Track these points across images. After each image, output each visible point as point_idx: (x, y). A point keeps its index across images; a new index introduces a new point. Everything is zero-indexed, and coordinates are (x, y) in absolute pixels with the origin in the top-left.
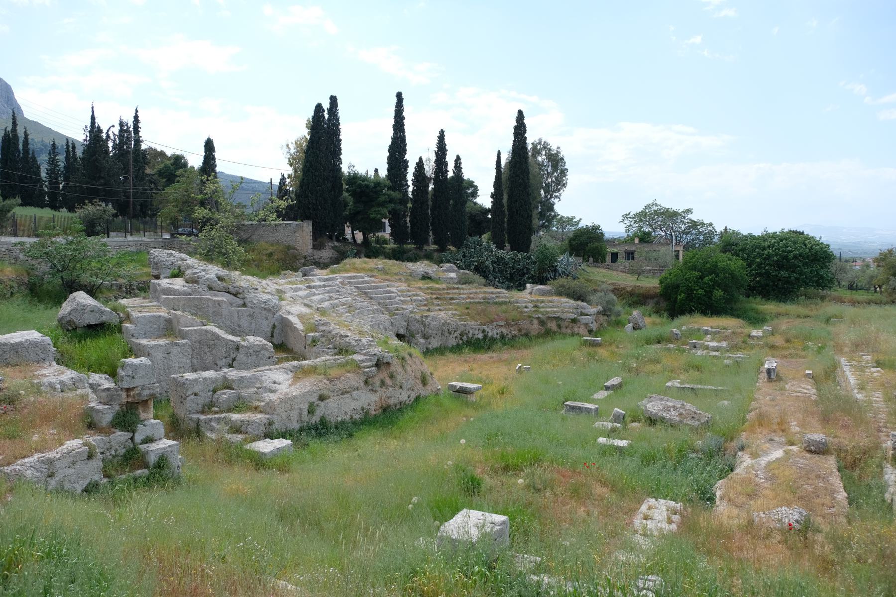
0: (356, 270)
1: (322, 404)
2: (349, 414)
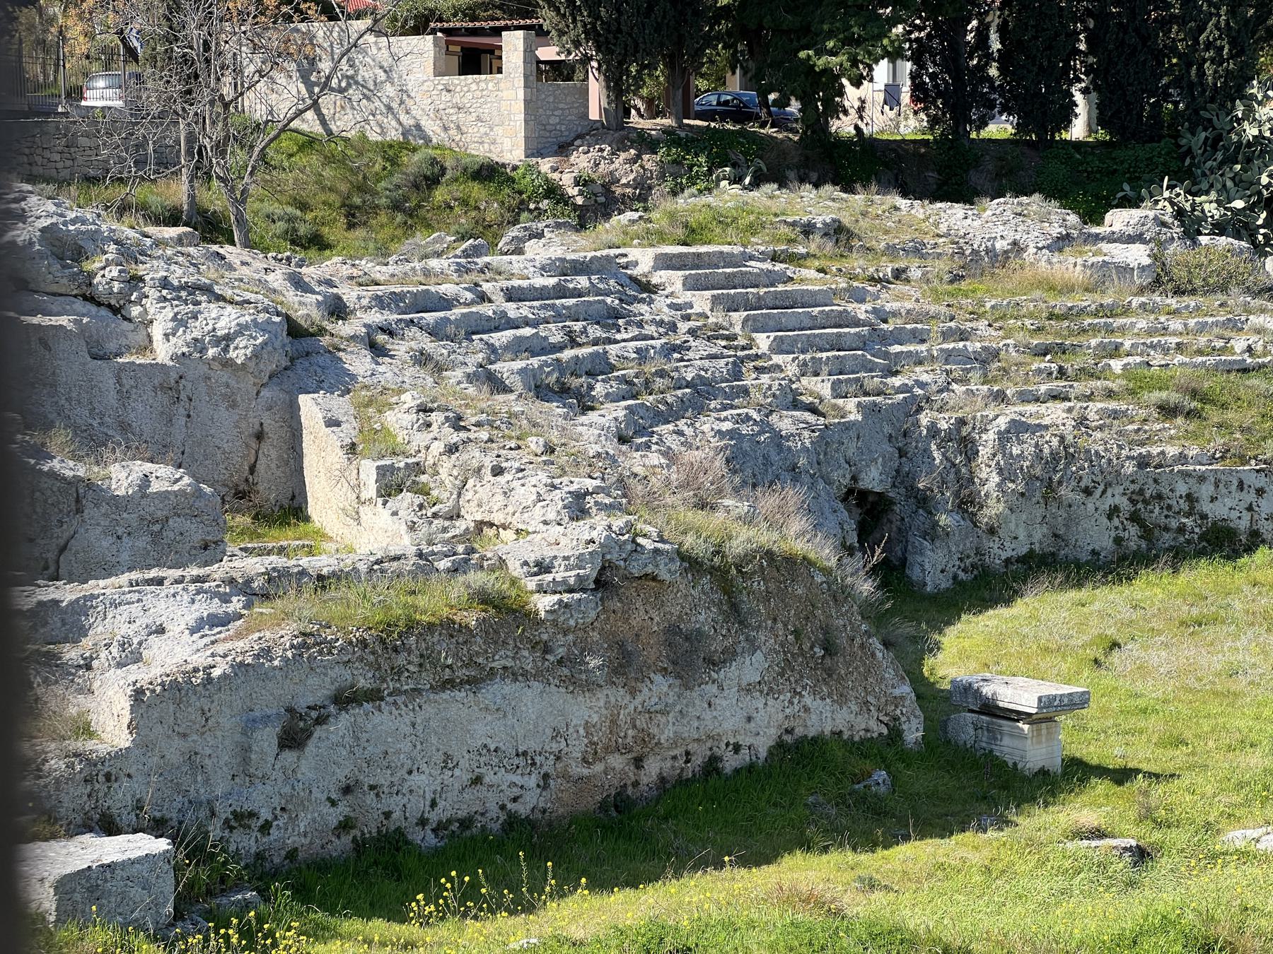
2: (464, 763)
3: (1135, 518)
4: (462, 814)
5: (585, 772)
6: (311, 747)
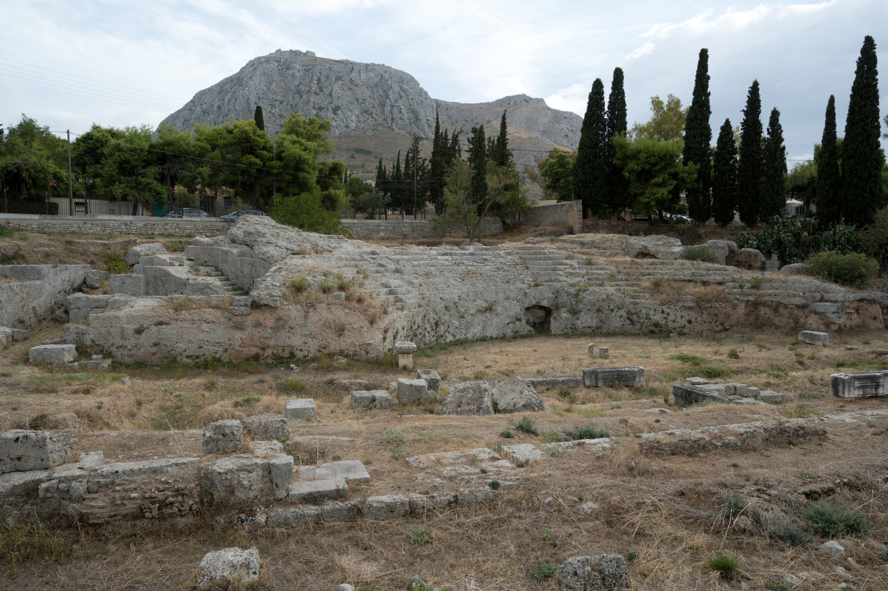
1: (154, 329)
3: (628, 319)
5: (241, 349)
6: (143, 334)
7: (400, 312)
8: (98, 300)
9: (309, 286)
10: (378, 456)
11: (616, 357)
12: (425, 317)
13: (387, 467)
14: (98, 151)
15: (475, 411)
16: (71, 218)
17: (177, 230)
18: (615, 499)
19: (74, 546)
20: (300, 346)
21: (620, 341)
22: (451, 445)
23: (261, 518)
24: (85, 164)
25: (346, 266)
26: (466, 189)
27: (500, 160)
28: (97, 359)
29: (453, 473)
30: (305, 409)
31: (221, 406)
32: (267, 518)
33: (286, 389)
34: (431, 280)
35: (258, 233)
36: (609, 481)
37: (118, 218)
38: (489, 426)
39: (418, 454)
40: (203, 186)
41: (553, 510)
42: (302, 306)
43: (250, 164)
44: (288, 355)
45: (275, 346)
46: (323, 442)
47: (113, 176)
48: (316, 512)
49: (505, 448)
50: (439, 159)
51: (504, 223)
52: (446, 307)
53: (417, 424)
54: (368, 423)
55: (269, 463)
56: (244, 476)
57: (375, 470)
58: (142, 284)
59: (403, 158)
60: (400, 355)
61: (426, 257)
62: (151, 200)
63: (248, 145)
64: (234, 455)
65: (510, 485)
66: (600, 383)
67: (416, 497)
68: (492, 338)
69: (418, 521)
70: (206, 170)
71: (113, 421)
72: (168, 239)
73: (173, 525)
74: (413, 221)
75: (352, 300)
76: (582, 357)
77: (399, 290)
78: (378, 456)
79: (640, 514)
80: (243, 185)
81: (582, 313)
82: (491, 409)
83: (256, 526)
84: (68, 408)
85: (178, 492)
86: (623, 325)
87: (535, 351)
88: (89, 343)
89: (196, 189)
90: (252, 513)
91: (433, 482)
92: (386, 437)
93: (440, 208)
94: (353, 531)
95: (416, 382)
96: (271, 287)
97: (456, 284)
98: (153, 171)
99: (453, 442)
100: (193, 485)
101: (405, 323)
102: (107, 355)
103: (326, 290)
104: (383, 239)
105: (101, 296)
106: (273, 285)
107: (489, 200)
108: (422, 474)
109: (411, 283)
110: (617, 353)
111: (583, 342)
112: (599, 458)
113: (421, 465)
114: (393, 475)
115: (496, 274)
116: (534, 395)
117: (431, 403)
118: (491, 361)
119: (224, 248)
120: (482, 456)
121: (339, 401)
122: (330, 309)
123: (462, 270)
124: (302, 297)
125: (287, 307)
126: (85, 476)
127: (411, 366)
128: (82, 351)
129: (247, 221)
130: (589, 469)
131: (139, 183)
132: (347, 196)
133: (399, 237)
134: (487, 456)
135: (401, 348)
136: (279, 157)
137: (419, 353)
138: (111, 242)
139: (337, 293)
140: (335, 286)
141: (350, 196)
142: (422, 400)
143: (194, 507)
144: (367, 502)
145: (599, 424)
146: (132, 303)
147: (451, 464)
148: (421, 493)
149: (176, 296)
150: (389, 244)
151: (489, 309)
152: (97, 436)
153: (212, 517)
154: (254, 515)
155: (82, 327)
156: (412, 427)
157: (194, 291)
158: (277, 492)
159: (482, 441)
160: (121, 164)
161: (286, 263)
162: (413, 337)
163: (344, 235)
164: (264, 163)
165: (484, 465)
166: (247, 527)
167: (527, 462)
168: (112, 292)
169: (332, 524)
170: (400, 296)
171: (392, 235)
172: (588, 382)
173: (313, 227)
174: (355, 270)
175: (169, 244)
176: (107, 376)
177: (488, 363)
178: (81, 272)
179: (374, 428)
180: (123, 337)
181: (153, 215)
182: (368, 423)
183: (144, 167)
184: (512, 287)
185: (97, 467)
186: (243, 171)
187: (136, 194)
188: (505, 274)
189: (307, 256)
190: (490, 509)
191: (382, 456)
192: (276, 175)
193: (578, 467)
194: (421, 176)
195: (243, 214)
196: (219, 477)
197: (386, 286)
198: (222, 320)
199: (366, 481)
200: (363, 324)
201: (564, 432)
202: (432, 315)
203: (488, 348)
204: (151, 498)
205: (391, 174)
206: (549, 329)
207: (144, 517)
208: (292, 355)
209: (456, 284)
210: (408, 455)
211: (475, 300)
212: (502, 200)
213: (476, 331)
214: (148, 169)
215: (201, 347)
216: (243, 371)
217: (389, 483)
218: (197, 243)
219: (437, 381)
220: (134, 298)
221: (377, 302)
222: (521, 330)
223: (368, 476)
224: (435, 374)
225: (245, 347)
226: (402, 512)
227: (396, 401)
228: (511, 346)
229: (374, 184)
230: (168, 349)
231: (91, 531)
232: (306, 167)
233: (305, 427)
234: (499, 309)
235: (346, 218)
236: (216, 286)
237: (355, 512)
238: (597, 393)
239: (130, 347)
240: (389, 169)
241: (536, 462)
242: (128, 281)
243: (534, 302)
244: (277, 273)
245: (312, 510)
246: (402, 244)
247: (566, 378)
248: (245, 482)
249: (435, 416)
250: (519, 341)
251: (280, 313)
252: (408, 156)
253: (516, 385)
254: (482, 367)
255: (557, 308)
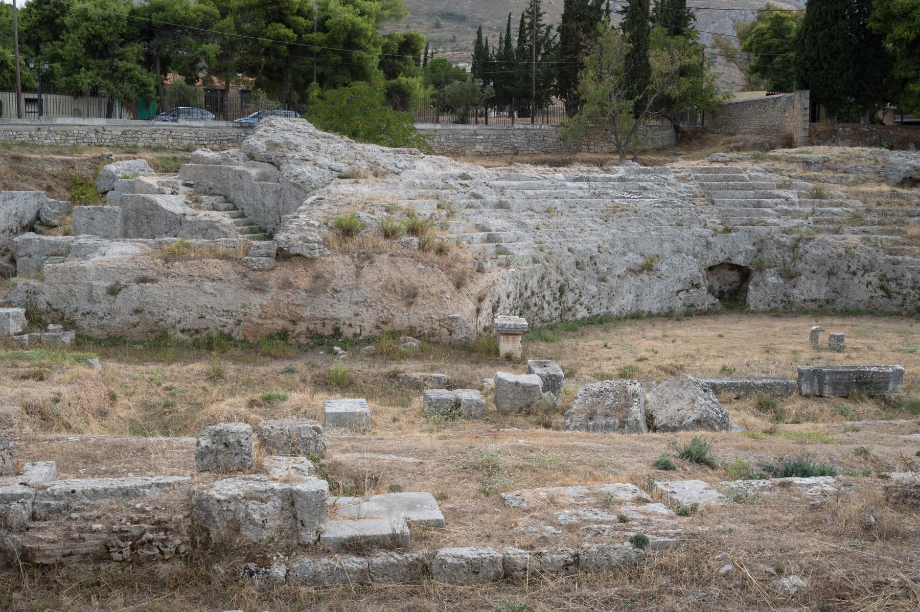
0: (776, 158)
1: (135, 287)
3: (882, 288)
4: (196, 327)
5: (260, 322)
6: (120, 295)
7: (503, 270)
8: (56, 244)
9: (364, 226)
10: (458, 488)
11: (856, 350)
12: (543, 278)
13: (471, 505)
14: (58, 21)
15: (616, 426)
16: (20, 121)
17: (170, 140)
18: (838, 573)
19: (15, 595)
20: (349, 319)
21: (865, 323)
22: (574, 476)
23: (279, 571)
24: (39, 40)
25: (421, 196)
26: (617, 74)
27: (673, 26)
28: (54, 331)
29: (574, 520)
30: (353, 414)
31: (230, 405)
32: (288, 571)
33: (326, 384)
34: (554, 220)
35: (288, 143)
36: (829, 545)
37: (86, 122)
38: (636, 451)
39: (521, 487)
40: (210, 72)
41: (732, 585)
42: (353, 257)
43: (279, 39)
44: (331, 332)
45: (313, 318)
46: (375, 463)
47: (77, 58)
48: (360, 567)
49: (660, 485)
50: (574, 25)
51: (677, 129)
52: (577, 264)
53: (521, 442)
54: (446, 438)
55: (291, 490)
56: (255, 507)
57: (453, 509)
58: (119, 220)
59: (515, 26)
60: (502, 338)
61: (547, 183)
62: (133, 95)
63: (275, 7)
64: (240, 475)
65: (665, 542)
66: (827, 391)
67: (514, 552)
68: (650, 315)
69: (515, 589)
70: (213, 48)
71: (73, 421)
72: (156, 154)
73: (151, 573)
74: (530, 127)
75: (429, 250)
76: (799, 348)
77: (503, 235)
78: (458, 488)
79: (880, 600)
80: (268, 70)
81: (803, 277)
82: (643, 425)
83: (271, 582)
84: (13, 399)
85: (160, 525)
86: (872, 297)
87: (721, 336)
88: (43, 306)
89: (198, 78)
90: (265, 562)
91: (542, 530)
92: (472, 460)
93: (574, 105)
94: (415, 598)
95: (524, 379)
96: (306, 228)
97: (595, 226)
98: (136, 50)
99: (576, 472)
100: (181, 516)
101: (511, 288)
102: (69, 325)
103: (389, 234)
104: (480, 155)
105: (60, 238)
106: (309, 225)
107: (654, 92)
108: (526, 518)
109: (522, 225)
110: (859, 342)
111: (801, 324)
112: (814, 507)
113: (524, 505)
114: (481, 517)
115: (660, 212)
116: (714, 406)
117: (546, 412)
118: (647, 351)
119: (238, 168)
120: (622, 495)
121: (405, 403)
122: (394, 262)
123: (605, 205)
124: (353, 244)
125: (329, 259)
126: (30, 496)
127: (518, 354)
128: (35, 319)
129: (272, 126)
130: (797, 523)
131: (116, 70)
132: (426, 87)
133: (507, 152)
134: (630, 496)
135: (503, 326)
136: (322, 27)
137: (531, 334)
138: (75, 157)
139: (405, 238)
140: (404, 227)
141: (431, 87)
142: (533, 407)
143: (183, 549)
144: (437, 557)
145: (819, 454)
146: (103, 250)
147: (571, 506)
148: (523, 548)
149: (167, 239)
150: (490, 164)
151: (648, 268)
152: (51, 441)
153: (208, 565)
154: (269, 566)
155: (34, 283)
156: (513, 447)
157: (193, 234)
158: (303, 533)
159: (623, 472)
160: (89, 40)
161: (329, 192)
162: (523, 309)
163: (419, 148)
164: (300, 36)
165: (624, 510)
166: (257, 582)
167: (694, 508)
168: (76, 233)
169: (384, 586)
170: (504, 244)
171: (495, 149)
172: (806, 389)
173: (371, 137)
174: (435, 203)
175: (159, 162)
176: (68, 355)
177: (643, 354)
178: (33, 202)
179: (455, 445)
180: (91, 299)
181: (135, 118)
182: (446, 438)
183: (122, 45)
184: (686, 233)
185: (46, 484)
186: (267, 49)
187: (112, 86)
188: (675, 211)
189: (361, 180)
190: (630, 578)
191: (466, 488)
192: (318, 54)
193: (779, 520)
194: (543, 55)
195: (267, 115)
196: (217, 507)
197: (483, 229)
198: (233, 276)
199: (438, 525)
200: (445, 288)
201: (759, 465)
202: (554, 276)
203: (643, 330)
204: (121, 531)
205: (496, 52)
206: (745, 301)
207: (111, 559)
208: (337, 333)
209: (595, 226)
210: (505, 488)
211: (624, 254)
212: (674, 91)
213: (625, 302)
214: (128, 48)
215: (202, 317)
216: (264, 355)
217: (473, 530)
218: (199, 160)
219: (558, 378)
220: (106, 242)
221: (468, 255)
222: (699, 302)
223: (441, 517)
224: (555, 368)
225: (266, 318)
226: (492, 574)
227: (493, 407)
228: (680, 327)
229: (469, 69)
230: (156, 319)
231: (38, 575)
232: (363, 42)
233: (349, 440)
234: (664, 268)
235: (424, 122)
236: (225, 226)
237: (419, 570)
238: (821, 406)
239: (100, 314)
240: (494, 43)
241: (709, 509)
242: (99, 216)
243: (721, 258)
244: (315, 207)
245: (354, 562)
246: (511, 164)
247: (769, 381)
248: (256, 516)
249: (551, 431)
250: (694, 321)
251: (319, 267)
252: (522, 22)
253: (685, 389)
254: (633, 360)
255: (761, 269)
